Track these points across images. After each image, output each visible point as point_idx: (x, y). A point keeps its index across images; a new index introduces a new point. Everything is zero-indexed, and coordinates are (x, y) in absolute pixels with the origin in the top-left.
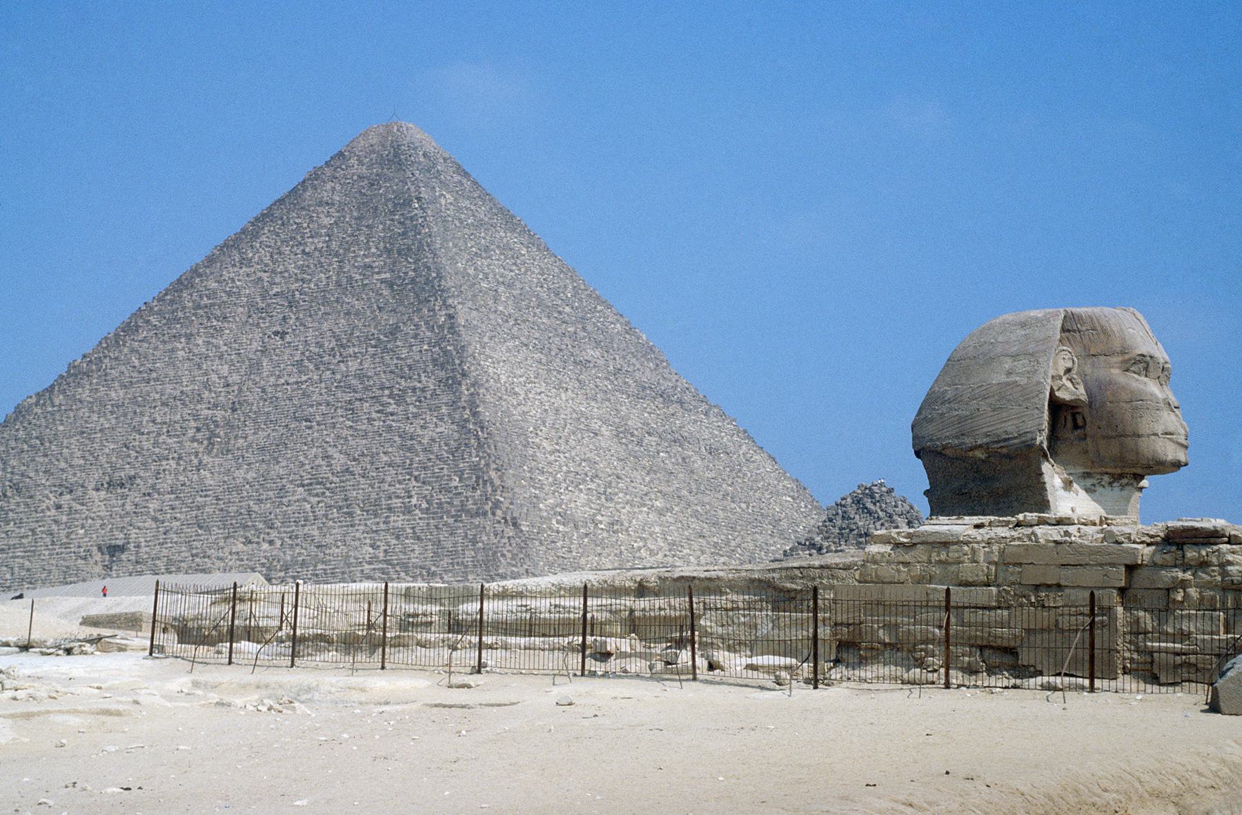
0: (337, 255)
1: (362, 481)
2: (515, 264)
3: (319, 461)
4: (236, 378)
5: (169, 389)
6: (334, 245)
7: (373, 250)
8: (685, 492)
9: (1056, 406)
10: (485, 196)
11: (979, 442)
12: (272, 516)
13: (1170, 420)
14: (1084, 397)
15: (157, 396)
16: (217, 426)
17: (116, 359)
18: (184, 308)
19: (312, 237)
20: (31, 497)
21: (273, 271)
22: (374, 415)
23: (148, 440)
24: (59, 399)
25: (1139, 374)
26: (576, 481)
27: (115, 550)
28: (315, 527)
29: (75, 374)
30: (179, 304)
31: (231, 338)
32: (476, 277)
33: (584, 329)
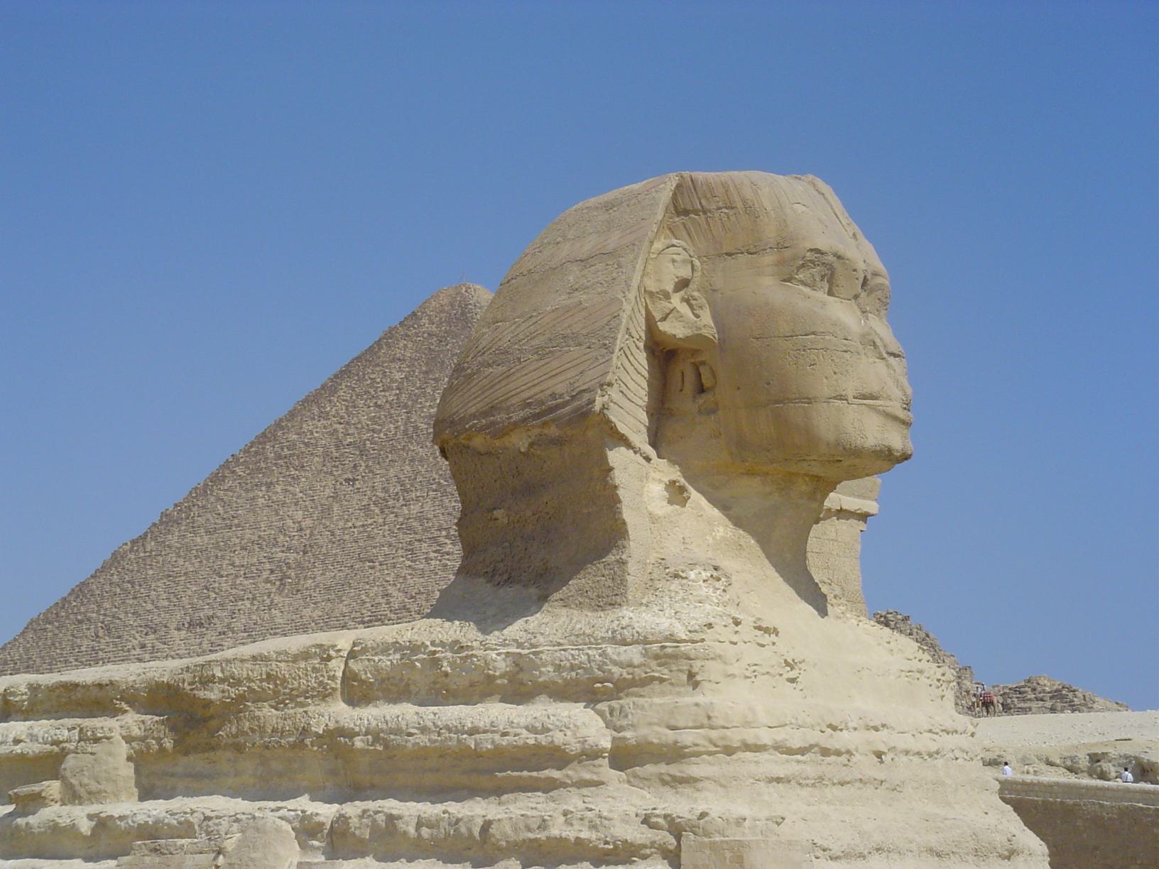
0: (406, 406)
3: (380, 600)
4: (308, 522)
5: (248, 534)
6: (404, 397)
9: (664, 354)
15: (237, 541)
16: (289, 568)
17: (203, 507)
18: (267, 458)
20: (119, 637)
21: (348, 423)
23: (226, 582)
24: (151, 545)
25: (812, 286)
29: (167, 520)
30: (266, 454)
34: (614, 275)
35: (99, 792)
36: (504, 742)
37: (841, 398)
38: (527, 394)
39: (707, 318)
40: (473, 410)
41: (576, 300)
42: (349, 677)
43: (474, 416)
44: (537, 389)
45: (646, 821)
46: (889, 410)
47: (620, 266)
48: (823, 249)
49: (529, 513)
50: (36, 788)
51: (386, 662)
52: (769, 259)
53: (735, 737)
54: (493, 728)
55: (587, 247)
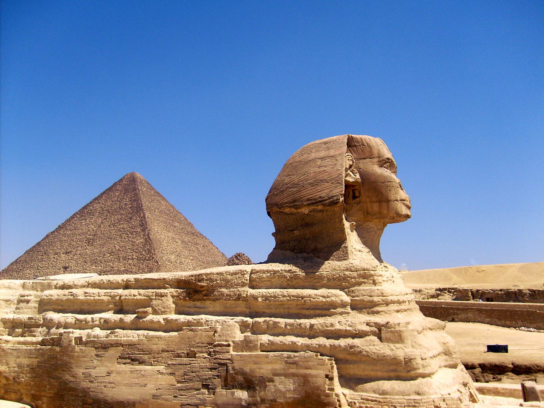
4: (95, 229)
5: (80, 231)
13: (402, 194)
14: (360, 180)
25: (387, 169)
26: (172, 253)
27: (66, 268)
29: (60, 227)
35: (165, 312)
37: (397, 200)
38: (310, 196)
39: (358, 176)
40: (286, 201)
43: (287, 203)
45: (368, 324)
49: (308, 232)
50: (145, 310)
52: (376, 160)
53: (390, 298)
54: (310, 296)
55: (322, 154)
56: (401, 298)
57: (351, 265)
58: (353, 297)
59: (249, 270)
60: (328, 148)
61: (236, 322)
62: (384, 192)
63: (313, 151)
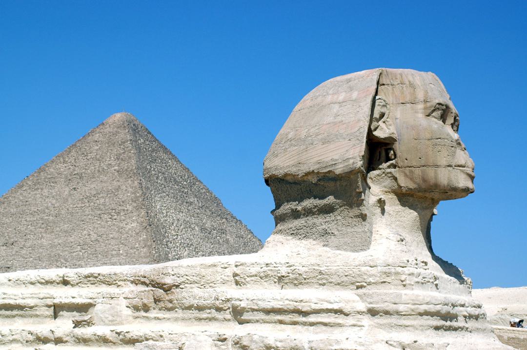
1: (102, 244)
2: (166, 166)
5: (33, 209)
6: (98, 157)
7: (112, 159)
8: (226, 252)
10: (156, 140)
11: (311, 169)
12: (67, 257)
14: (394, 136)
15: (28, 211)
19: (90, 153)
21: (75, 166)
22: (108, 220)
28: (83, 261)
31: (57, 190)
32: (150, 169)
33: (191, 190)
34: (358, 110)
36: (314, 307)
41: (340, 120)
42: (235, 275)
43: (289, 166)
44: (322, 157)
46: (468, 172)
47: (360, 106)
48: (443, 103)
51: (254, 270)
52: (421, 106)
56: (445, 309)
57: (371, 258)
58: (371, 303)
59: (233, 263)
60: (351, 89)
61: (210, 336)
62: (431, 153)
63: (331, 92)
